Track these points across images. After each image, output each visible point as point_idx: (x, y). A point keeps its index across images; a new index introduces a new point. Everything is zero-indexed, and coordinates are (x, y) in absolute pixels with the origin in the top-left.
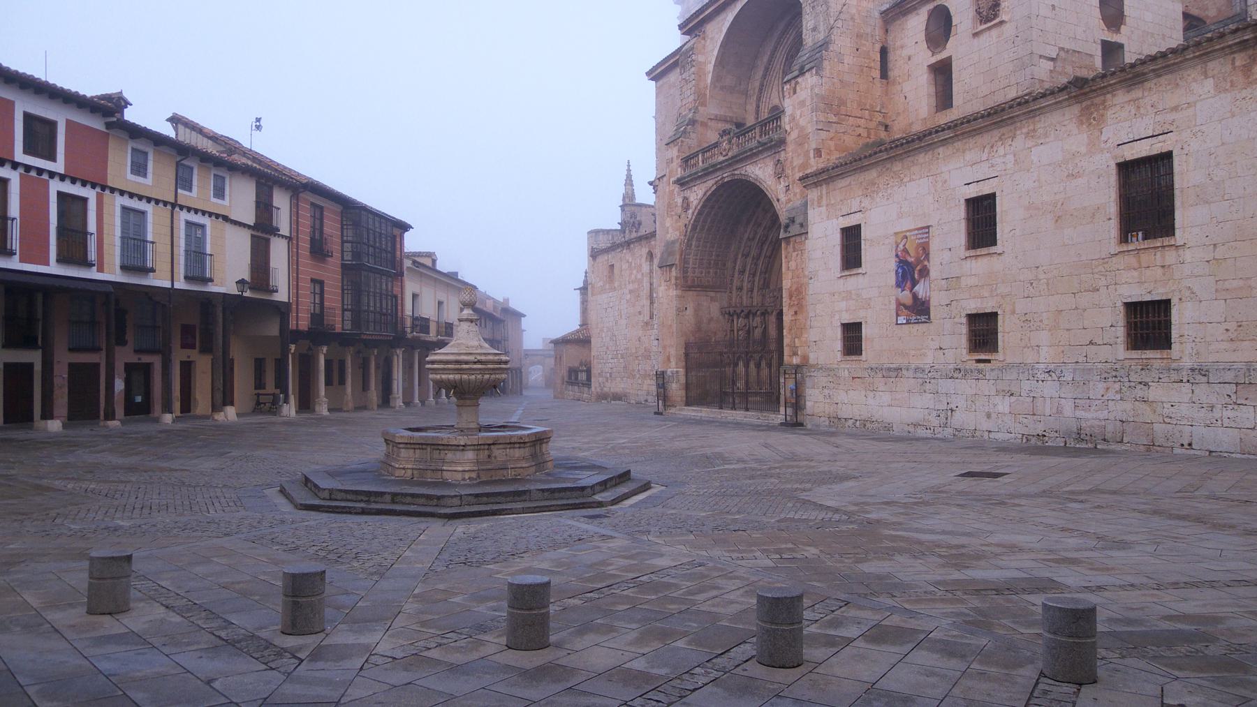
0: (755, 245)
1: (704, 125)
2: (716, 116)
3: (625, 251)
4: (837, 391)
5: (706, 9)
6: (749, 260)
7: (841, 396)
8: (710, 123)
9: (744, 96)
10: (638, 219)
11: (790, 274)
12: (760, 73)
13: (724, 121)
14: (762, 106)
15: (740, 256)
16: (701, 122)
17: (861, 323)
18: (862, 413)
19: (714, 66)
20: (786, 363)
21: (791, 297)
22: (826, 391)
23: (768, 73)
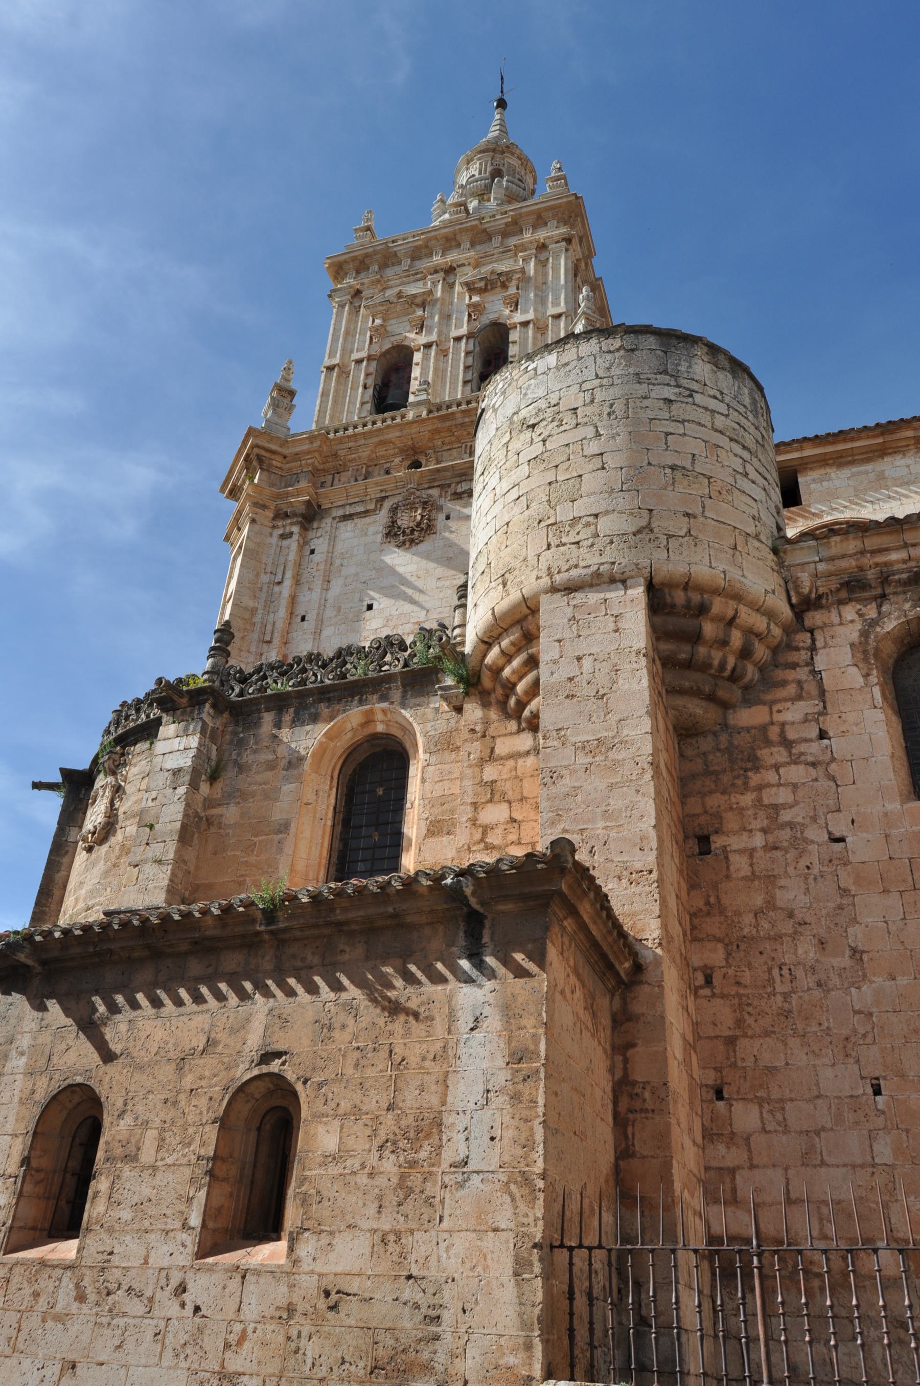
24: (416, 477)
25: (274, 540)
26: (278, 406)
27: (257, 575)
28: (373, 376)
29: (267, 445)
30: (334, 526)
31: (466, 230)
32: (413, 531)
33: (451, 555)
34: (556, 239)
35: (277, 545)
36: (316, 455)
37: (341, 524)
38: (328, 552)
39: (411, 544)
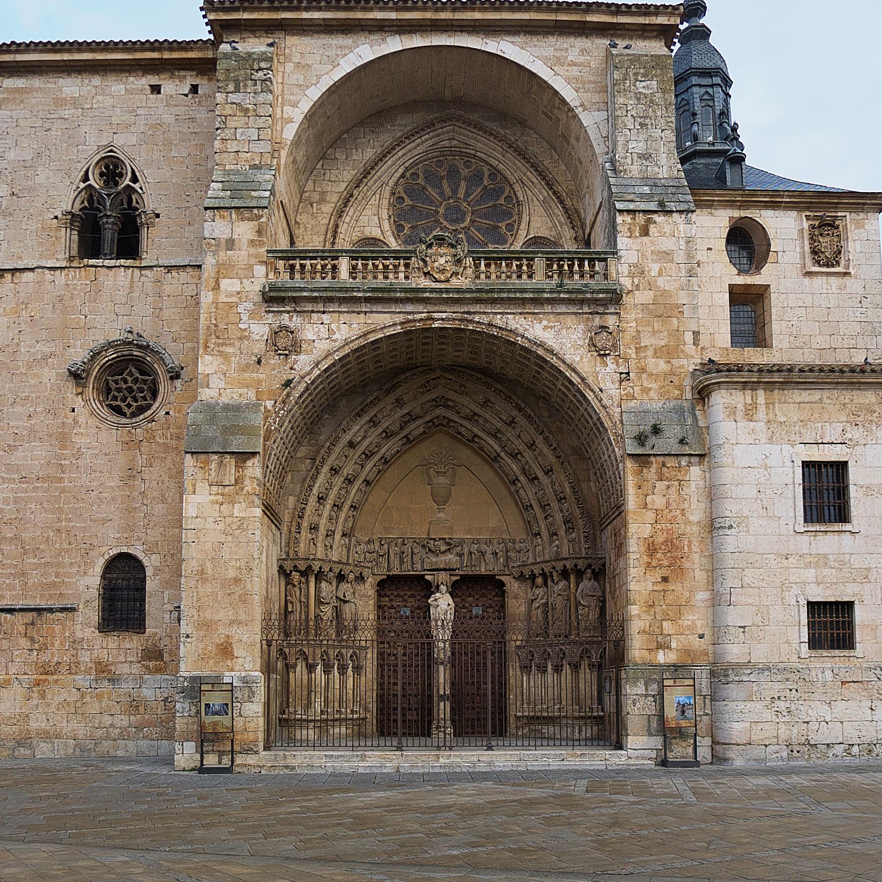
0: (356, 457)
4: (807, 703)
6: (339, 481)
7: (817, 710)
11: (650, 516)
12: (348, 174)
14: (343, 228)
15: (325, 469)
17: (853, 603)
18: (864, 733)
20: (639, 661)
21: (651, 550)
22: (782, 705)
23: (365, 180)
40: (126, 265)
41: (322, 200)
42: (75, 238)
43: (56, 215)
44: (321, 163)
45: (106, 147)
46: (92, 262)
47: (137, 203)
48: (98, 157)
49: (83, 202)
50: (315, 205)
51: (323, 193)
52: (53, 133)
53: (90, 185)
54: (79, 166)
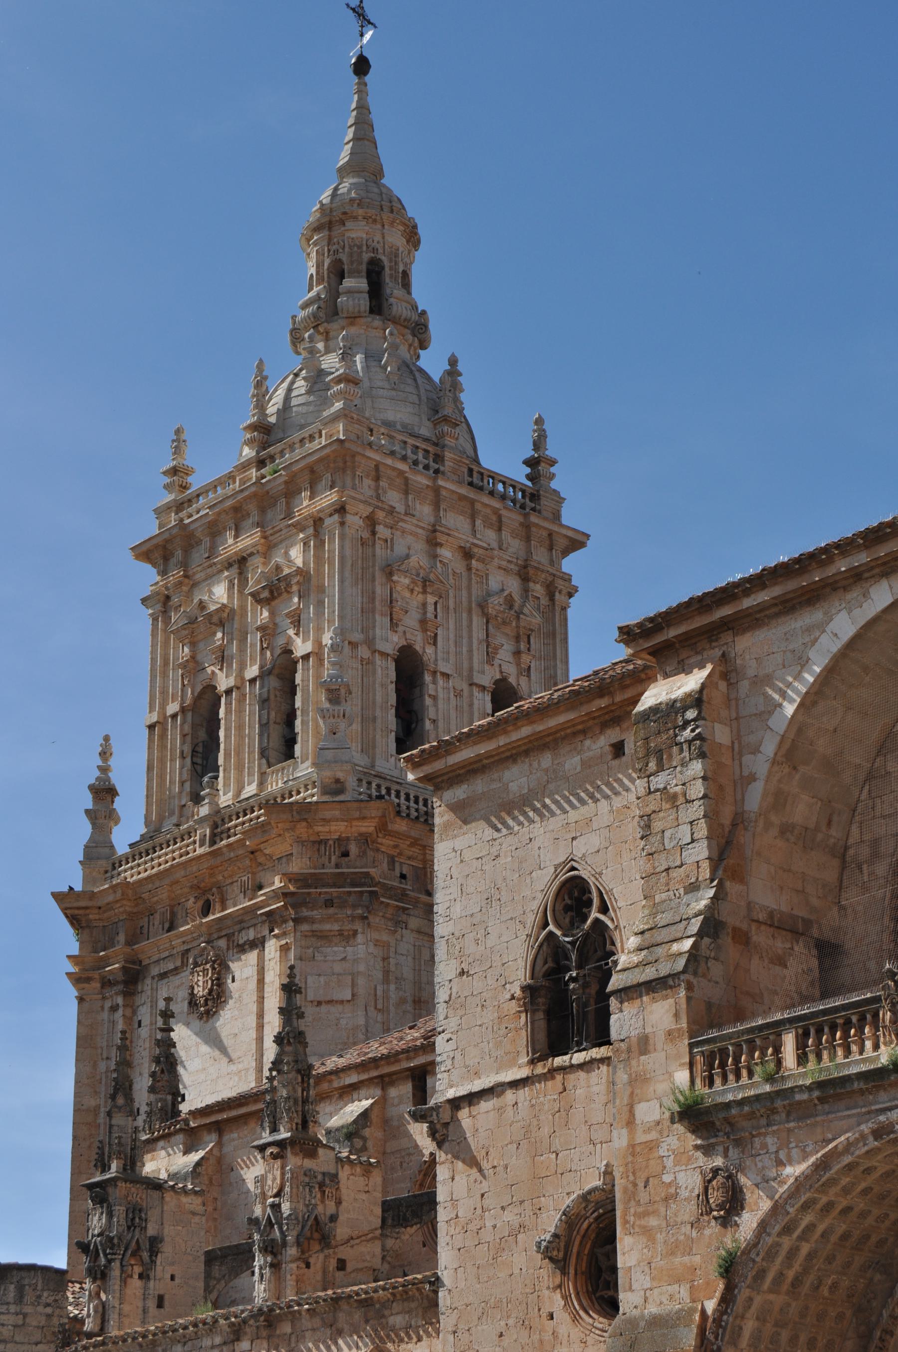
1: (742, 938)
2: (771, 914)
3: (245, 1345)
5: (747, 593)
8: (761, 937)
9: (836, 863)
10: (151, 1231)
13: (791, 931)
16: (735, 929)
19: (774, 762)
24: (204, 929)
25: (105, 1015)
26: (96, 818)
27: (95, 1066)
28: (190, 736)
29: (76, 905)
30: (155, 987)
31: (249, 497)
32: (206, 1000)
33: (237, 1031)
34: (328, 511)
35: (109, 1021)
36: (125, 902)
37: (160, 983)
38: (151, 1024)
39: (208, 1017)
40: (598, 1057)
41: (875, 855)
42: (542, 1024)
43: (512, 992)
44: (867, 787)
45: (565, 863)
46: (559, 1061)
47: (613, 943)
48: (557, 883)
49: (546, 962)
50: (865, 867)
51: (875, 843)
52: (502, 860)
53: (551, 933)
54: (535, 905)
